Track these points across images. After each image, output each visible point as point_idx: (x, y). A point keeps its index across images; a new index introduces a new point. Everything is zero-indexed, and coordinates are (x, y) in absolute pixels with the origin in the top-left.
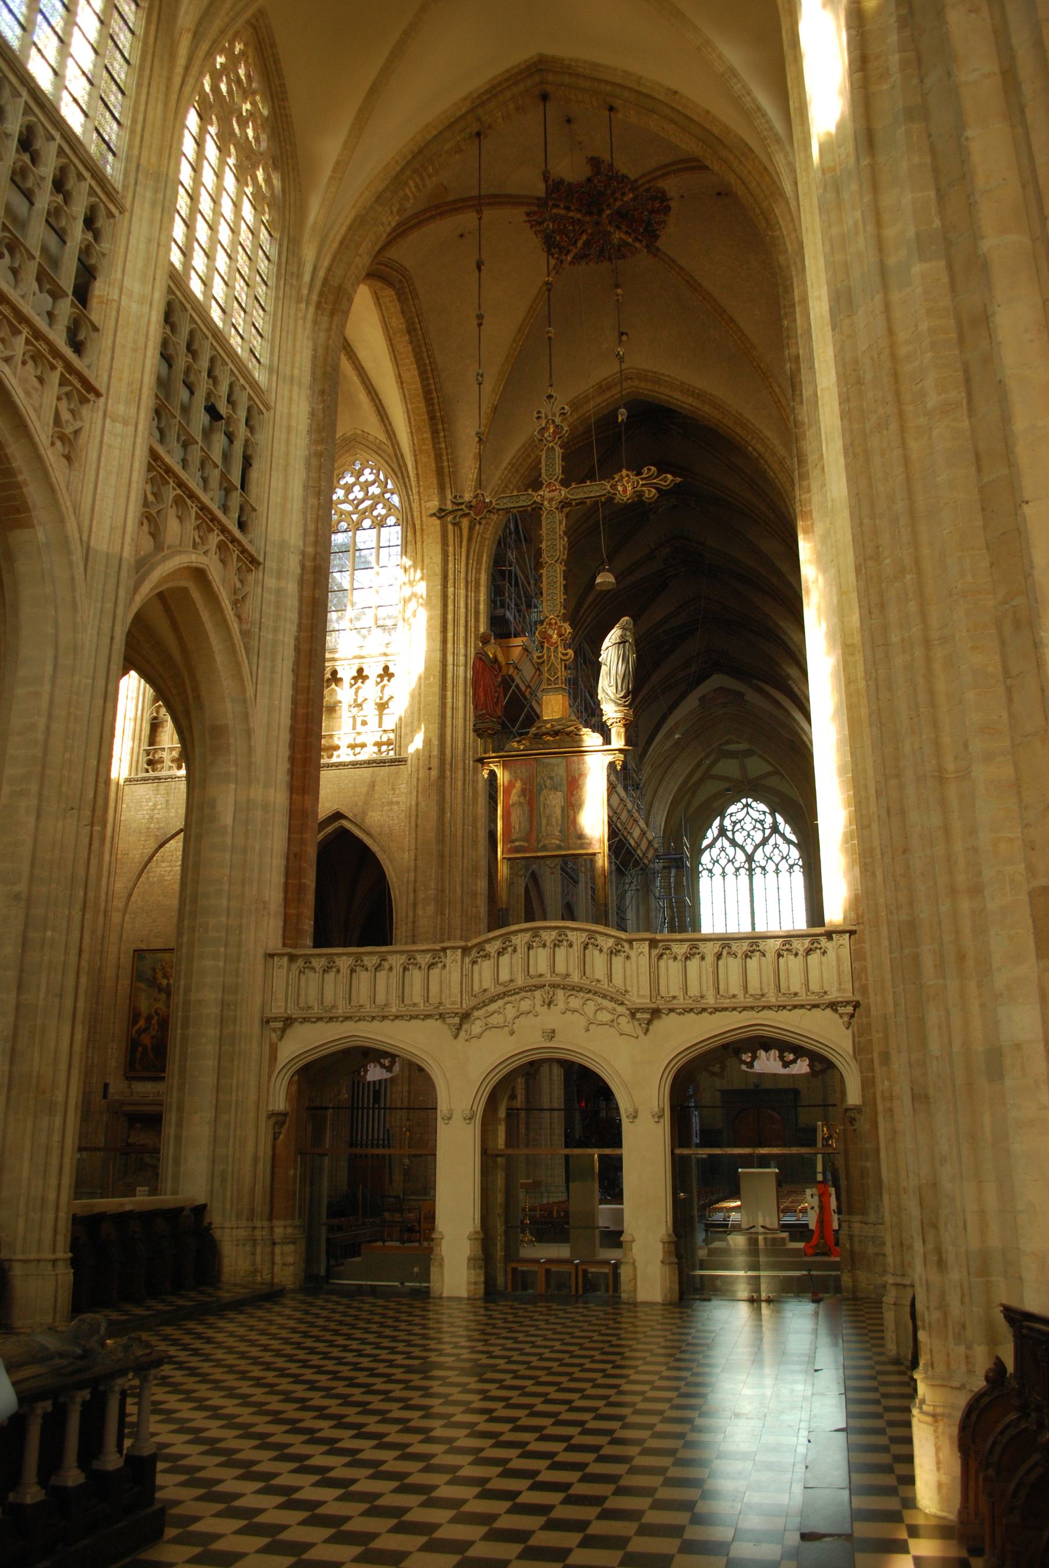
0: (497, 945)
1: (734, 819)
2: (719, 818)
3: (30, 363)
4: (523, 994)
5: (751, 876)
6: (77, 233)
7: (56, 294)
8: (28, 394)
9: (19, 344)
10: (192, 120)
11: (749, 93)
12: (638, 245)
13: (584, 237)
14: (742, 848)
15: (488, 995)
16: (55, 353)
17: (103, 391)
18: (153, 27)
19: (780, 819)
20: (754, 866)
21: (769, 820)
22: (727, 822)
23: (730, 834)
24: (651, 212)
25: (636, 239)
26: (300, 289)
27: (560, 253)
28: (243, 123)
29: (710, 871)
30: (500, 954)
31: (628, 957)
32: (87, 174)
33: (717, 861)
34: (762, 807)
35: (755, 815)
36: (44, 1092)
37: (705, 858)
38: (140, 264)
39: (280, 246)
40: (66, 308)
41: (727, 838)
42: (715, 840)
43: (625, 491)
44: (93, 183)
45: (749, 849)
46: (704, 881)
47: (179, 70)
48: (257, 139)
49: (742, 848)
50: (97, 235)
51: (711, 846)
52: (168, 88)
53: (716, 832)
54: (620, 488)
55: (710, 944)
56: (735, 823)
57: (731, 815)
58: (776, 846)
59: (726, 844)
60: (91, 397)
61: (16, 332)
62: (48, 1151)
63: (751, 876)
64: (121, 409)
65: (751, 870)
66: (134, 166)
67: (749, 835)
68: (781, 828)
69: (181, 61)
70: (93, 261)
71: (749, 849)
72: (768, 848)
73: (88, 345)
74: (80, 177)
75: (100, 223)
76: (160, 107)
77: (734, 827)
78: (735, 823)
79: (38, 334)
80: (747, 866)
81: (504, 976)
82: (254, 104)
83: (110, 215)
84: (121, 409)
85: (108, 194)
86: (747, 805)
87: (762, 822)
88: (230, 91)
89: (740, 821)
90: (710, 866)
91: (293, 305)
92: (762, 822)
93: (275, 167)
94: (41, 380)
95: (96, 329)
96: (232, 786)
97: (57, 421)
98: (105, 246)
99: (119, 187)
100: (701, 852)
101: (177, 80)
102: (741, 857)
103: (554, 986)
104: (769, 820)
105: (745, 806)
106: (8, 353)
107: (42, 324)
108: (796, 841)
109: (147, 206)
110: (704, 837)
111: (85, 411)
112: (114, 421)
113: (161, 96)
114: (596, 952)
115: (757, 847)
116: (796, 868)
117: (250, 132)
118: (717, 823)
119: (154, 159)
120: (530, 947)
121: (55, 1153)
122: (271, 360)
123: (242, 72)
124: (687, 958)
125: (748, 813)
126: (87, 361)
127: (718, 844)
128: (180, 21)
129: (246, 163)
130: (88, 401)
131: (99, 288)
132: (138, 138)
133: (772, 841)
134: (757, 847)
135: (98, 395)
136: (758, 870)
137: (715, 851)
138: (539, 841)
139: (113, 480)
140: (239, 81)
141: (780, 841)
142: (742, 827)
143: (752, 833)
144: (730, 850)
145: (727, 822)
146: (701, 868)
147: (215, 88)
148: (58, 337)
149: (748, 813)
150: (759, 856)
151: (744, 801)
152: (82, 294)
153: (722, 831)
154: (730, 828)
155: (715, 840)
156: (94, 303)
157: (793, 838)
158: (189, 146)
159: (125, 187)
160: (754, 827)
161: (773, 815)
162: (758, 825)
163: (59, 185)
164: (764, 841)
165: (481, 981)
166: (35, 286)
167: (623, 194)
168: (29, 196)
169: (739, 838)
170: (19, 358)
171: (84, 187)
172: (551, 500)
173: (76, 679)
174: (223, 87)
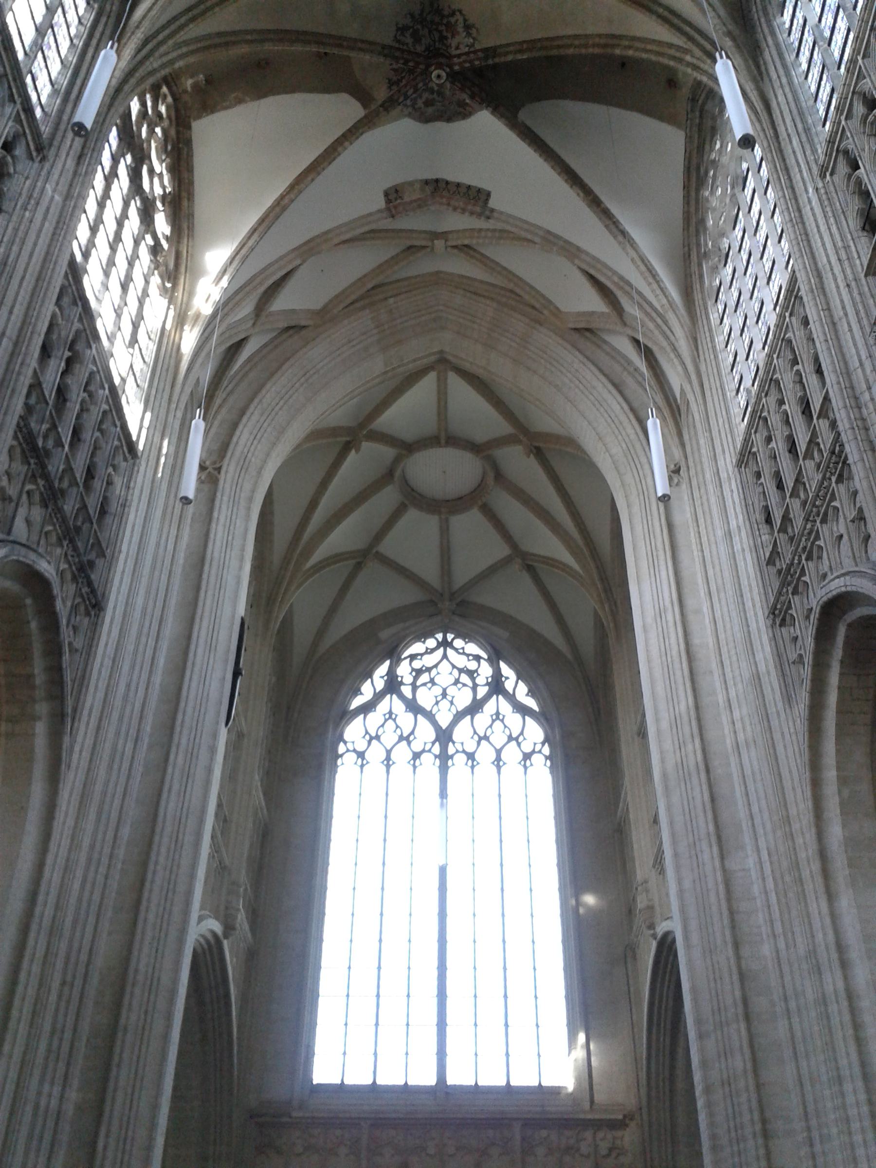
1: (417, 664)
2: (387, 663)
5: (444, 770)
14: (430, 717)
20: (451, 750)
21: (486, 671)
22: (404, 670)
23: (407, 691)
29: (361, 755)
33: (378, 738)
34: (473, 648)
35: (461, 661)
41: (401, 697)
42: (378, 697)
45: (444, 720)
49: (430, 717)
51: (367, 708)
53: (380, 684)
56: (419, 672)
57: (413, 657)
58: (497, 716)
59: (398, 706)
63: (444, 770)
65: (444, 758)
67: (444, 695)
68: (509, 686)
71: (444, 720)
72: (482, 720)
77: (416, 678)
80: (436, 749)
86: (445, 644)
89: (429, 670)
92: (471, 674)
100: (346, 716)
102: (425, 733)
104: (486, 671)
105: (439, 645)
108: (535, 707)
110: (357, 692)
118: (383, 669)
125: (445, 656)
127: (383, 706)
133: (490, 707)
134: (459, 717)
136: (460, 759)
137: (375, 719)
141: (505, 707)
142: (432, 681)
143: (452, 691)
144: (406, 720)
145: (404, 670)
146: (341, 748)
149: (445, 656)
150: (463, 733)
151: (440, 636)
153: (393, 685)
155: (378, 697)
157: (531, 703)
160: (457, 682)
161: (493, 661)
162: (465, 678)
164: (475, 707)
169: (425, 698)
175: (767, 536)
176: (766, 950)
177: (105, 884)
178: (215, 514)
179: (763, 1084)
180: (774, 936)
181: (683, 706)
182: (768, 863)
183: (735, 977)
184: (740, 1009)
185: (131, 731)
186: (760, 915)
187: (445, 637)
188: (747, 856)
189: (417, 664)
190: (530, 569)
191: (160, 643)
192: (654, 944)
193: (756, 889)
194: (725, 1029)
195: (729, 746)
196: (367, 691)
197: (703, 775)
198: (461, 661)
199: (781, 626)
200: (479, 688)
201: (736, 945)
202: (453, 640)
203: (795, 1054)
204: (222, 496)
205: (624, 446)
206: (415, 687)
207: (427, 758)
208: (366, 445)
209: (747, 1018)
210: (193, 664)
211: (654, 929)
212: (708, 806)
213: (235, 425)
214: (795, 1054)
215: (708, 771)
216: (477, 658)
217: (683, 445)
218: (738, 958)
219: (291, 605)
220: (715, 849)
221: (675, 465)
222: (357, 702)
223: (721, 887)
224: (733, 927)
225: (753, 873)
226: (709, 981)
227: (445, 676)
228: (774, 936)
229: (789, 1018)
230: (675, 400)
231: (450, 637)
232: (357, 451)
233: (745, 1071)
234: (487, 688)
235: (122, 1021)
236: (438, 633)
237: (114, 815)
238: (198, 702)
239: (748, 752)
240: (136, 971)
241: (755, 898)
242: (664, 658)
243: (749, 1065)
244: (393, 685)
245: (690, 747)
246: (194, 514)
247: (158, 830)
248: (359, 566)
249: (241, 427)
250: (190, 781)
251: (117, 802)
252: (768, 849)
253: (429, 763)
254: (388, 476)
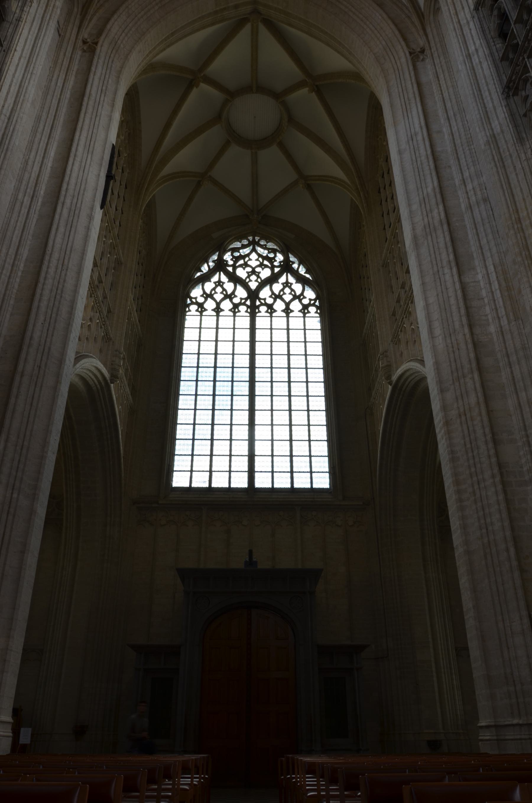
1: (237, 254)
14: (245, 285)
21: (280, 257)
22: (228, 257)
34: (270, 245)
35: (265, 253)
37: (196, 293)
41: (227, 273)
45: (253, 285)
49: (245, 285)
57: (234, 250)
71: (253, 285)
72: (277, 287)
77: (235, 263)
78: (236, 259)
80: (248, 303)
87: (271, 260)
102: (241, 293)
104: (280, 257)
115: (263, 284)
116: (312, 309)
118: (215, 257)
133: (283, 279)
136: (263, 309)
137: (209, 286)
144: (229, 287)
145: (228, 257)
154: (231, 263)
162: (266, 262)
164: (273, 279)
169: (241, 273)
175: (500, 45)
176: (492, 329)
177: (8, 282)
178: (93, 69)
179: (492, 411)
180: (499, 318)
181: (430, 189)
182: (494, 274)
183: (470, 346)
184: (474, 365)
185: (28, 190)
186: (487, 308)
187: (254, 239)
188: (477, 274)
189: (237, 254)
190: (309, 187)
191: (51, 140)
192: (390, 387)
193: (484, 293)
194: (462, 381)
195: (463, 206)
196: (205, 268)
197: (445, 227)
198: (265, 253)
199: (513, 95)
200: (275, 269)
201: (471, 326)
202: (259, 240)
203: (516, 389)
204: (98, 59)
205: (384, 43)
206: (235, 267)
207: (243, 308)
208: (203, 85)
209: (480, 369)
210: (75, 156)
211: (391, 378)
212: (449, 244)
213: (108, 20)
214: (516, 389)
215: (449, 224)
216: (274, 251)
217: (426, 35)
218: (472, 334)
219: (154, 196)
220: (455, 270)
221: (421, 49)
223: (459, 293)
224: (468, 315)
225: (482, 284)
226: (448, 353)
228: (499, 318)
229: (511, 367)
230: (420, 8)
231: (257, 239)
232: (197, 88)
233: (478, 403)
234: (279, 269)
235: (20, 368)
236: (250, 236)
237: (16, 240)
238: (79, 180)
239: (479, 207)
240: (31, 338)
241: (483, 299)
242: (415, 164)
243: (481, 400)
244: (221, 266)
245: (436, 211)
246: (78, 70)
247: (48, 252)
248: (199, 184)
249: (112, 20)
250: (73, 229)
251: (18, 232)
252: (494, 264)
254: (218, 118)
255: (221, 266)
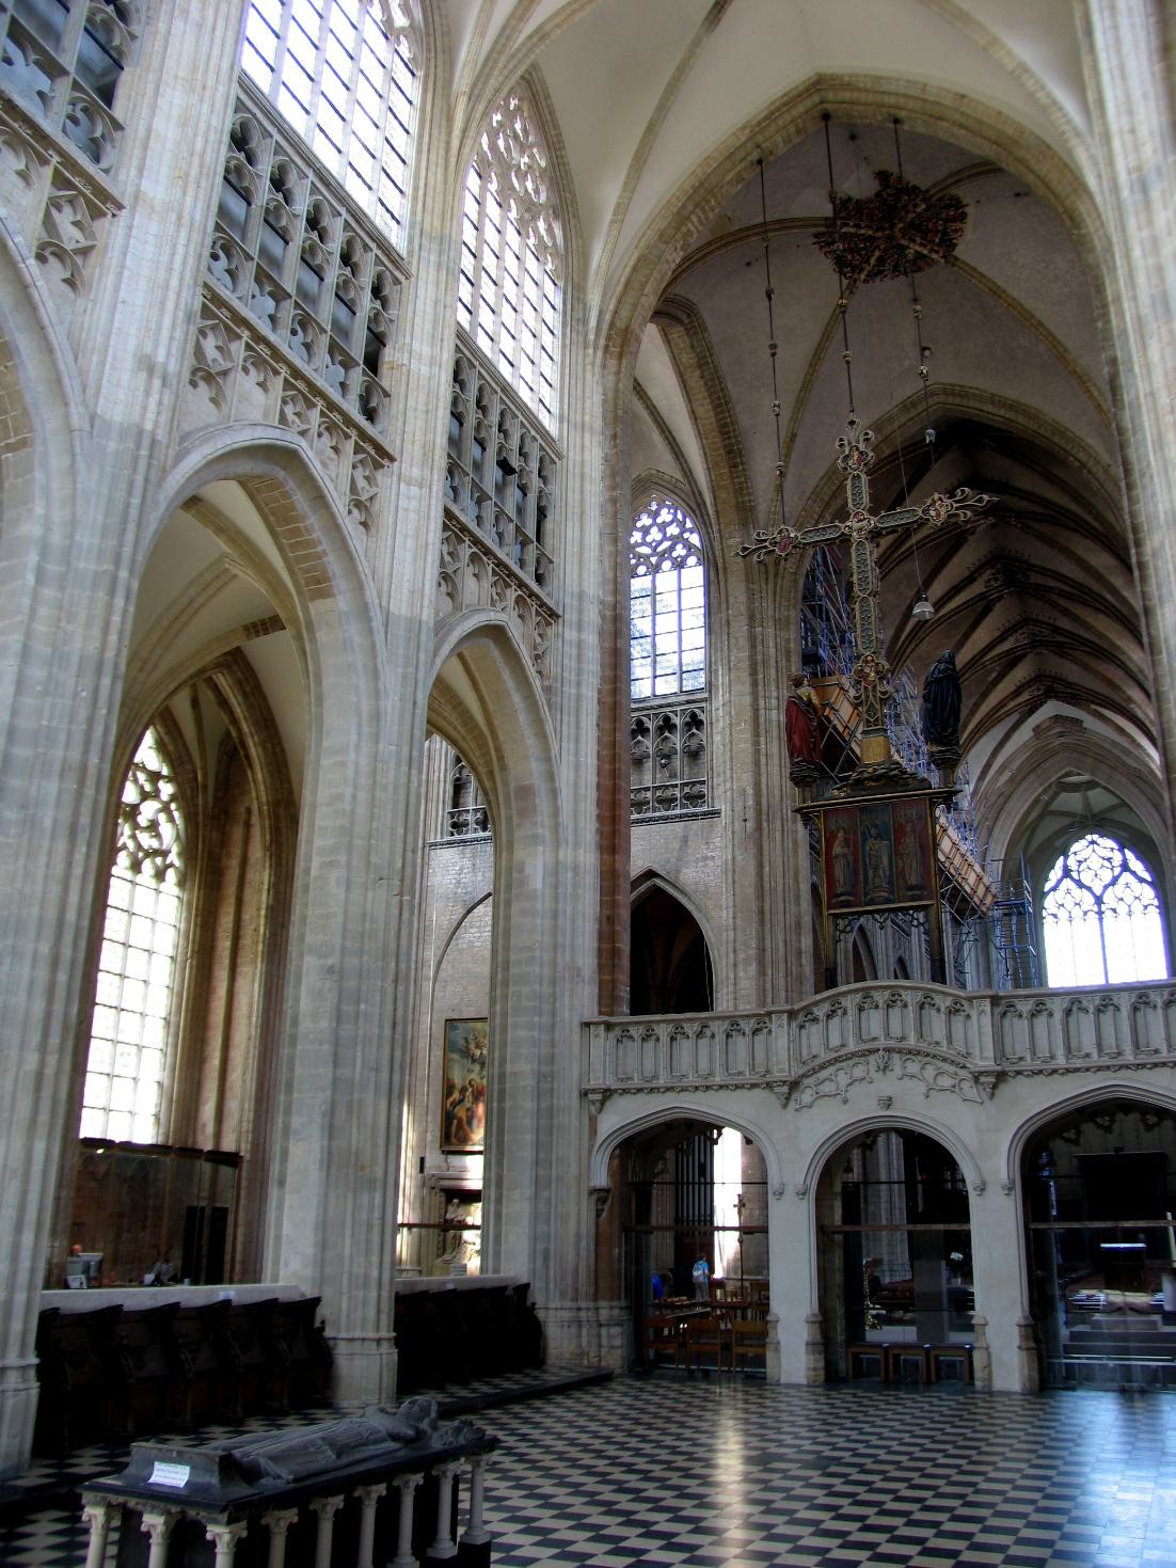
0: (826, 1007)
1: (1079, 858)
3: (326, 434)
4: (856, 1060)
5: (1101, 919)
6: (366, 303)
7: (347, 364)
8: (324, 465)
9: (314, 417)
10: (473, 181)
11: (1043, 88)
12: (934, 256)
13: (877, 253)
14: (1089, 889)
15: (818, 1062)
16: (349, 421)
17: (396, 455)
18: (430, 95)
19: (1129, 855)
21: (1117, 858)
22: (1072, 862)
23: (1075, 875)
24: (947, 220)
25: (932, 250)
26: (586, 335)
27: (853, 272)
28: (522, 177)
30: (829, 1017)
31: (968, 1017)
32: (373, 245)
34: (1110, 843)
36: (363, 1168)
38: (428, 326)
39: (565, 293)
40: (357, 377)
42: (1059, 882)
43: (938, 515)
44: (379, 253)
46: (1048, 923)
47: (457, 133)
48: (537, 191)
50: (384, 303)
51: (1054, 889)
52: (447, 151)
54: (933, 513)
55: (1057, 1000)
58: (1127, 886)
60: (385, 462)
61: (310, 405)
62: (370, 1227)
63: (1101, 919)
64: (416, 472)
65: (1100, 913)
66: (417, 231)
69: (458, 124)
70: (382, 329)
72: (1119, 888)
73: (380, 412)
74: (366, 248)
75: (386, 292)
76: (440, 171)
79: (332, 406)
81: (835, 1041)
82: (531, 157)
83: (397, 282)
84: (416, 472)
85: (393, 262)
86: (1093, 842)
88: (508, 148)
90: (1055, 911)
91: (581, 352)
93: (556, 217)
94: (335, 449)
95: (387, 395)
96: (541, 848)
97: (354, 489)
98: (393, 312)
99: (404, 253)
101: (455, 143)
102: (1089, 900)
103: (888, 1050)
104: (1117, 858)
106: (304, 427)
107: (335, 395)
109: (432, 269)
111: (379, 475)
112: (409, 484)
113: (441, 161)
114: (934, 1012)
117: (529, 185)
118: (1060, 862)
119: (437, 223)
120: (861, 1009)
121: (377, 1230)
122: (561, 408)
123: (518, 126)
124: (1033, 1015)
126: (379, 427)
128: (455, 86)
129: (527, 216)
130: (382, 466)
131: (388, 355)
132: (420, 204)
133: (1122, 881)
134: (1106, 887)
135: (392, 459)
137: (1059, 896)
138: (866, 894)
139: (410, 542)
140: (516, 136)
145: (1072, 862)
146: (1044, 913)
147: (493, 146)
148: (352, 407)
150: (1109, 897)
151: (1089, 837)
152: (372, 363)
153: (1067, 873)
155: (1059, 882)
156: (384, 370)
157: (1147, 877)
158: (471, 207)
159: (410, 253)
161: (1121, 850)
162: (1106, 863)
163: (346, 259)
164: (1114, 881)
165: (809, 1046)
166: (328, 357)
167: (916, 206)
168: (318, 273)
169: (1086, 879)
170: (315, 429)
171: (370, 257)
172: (861, 529)
173: (381, 746)
174: (501, 143)
196: (1055, 874)
222: (1048, 886)
227: (1095, 862)
253: (1093, 917)
255: (1067, 873)
